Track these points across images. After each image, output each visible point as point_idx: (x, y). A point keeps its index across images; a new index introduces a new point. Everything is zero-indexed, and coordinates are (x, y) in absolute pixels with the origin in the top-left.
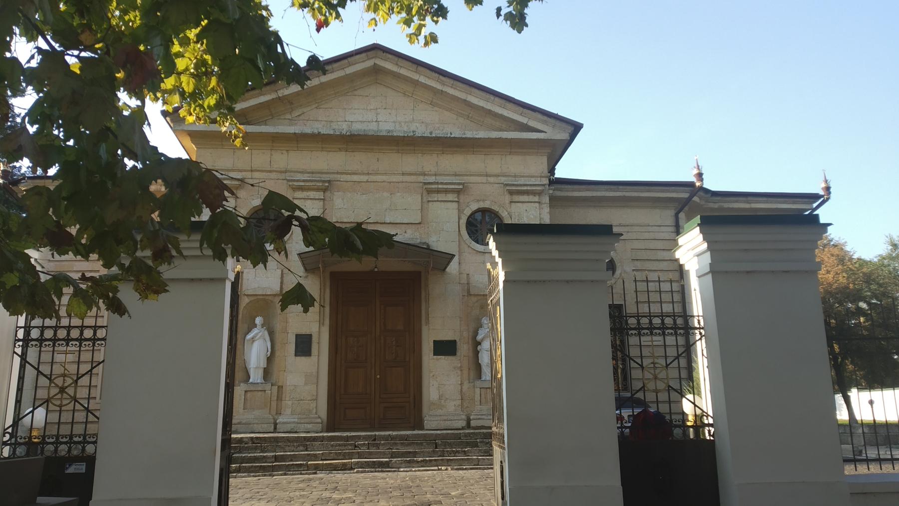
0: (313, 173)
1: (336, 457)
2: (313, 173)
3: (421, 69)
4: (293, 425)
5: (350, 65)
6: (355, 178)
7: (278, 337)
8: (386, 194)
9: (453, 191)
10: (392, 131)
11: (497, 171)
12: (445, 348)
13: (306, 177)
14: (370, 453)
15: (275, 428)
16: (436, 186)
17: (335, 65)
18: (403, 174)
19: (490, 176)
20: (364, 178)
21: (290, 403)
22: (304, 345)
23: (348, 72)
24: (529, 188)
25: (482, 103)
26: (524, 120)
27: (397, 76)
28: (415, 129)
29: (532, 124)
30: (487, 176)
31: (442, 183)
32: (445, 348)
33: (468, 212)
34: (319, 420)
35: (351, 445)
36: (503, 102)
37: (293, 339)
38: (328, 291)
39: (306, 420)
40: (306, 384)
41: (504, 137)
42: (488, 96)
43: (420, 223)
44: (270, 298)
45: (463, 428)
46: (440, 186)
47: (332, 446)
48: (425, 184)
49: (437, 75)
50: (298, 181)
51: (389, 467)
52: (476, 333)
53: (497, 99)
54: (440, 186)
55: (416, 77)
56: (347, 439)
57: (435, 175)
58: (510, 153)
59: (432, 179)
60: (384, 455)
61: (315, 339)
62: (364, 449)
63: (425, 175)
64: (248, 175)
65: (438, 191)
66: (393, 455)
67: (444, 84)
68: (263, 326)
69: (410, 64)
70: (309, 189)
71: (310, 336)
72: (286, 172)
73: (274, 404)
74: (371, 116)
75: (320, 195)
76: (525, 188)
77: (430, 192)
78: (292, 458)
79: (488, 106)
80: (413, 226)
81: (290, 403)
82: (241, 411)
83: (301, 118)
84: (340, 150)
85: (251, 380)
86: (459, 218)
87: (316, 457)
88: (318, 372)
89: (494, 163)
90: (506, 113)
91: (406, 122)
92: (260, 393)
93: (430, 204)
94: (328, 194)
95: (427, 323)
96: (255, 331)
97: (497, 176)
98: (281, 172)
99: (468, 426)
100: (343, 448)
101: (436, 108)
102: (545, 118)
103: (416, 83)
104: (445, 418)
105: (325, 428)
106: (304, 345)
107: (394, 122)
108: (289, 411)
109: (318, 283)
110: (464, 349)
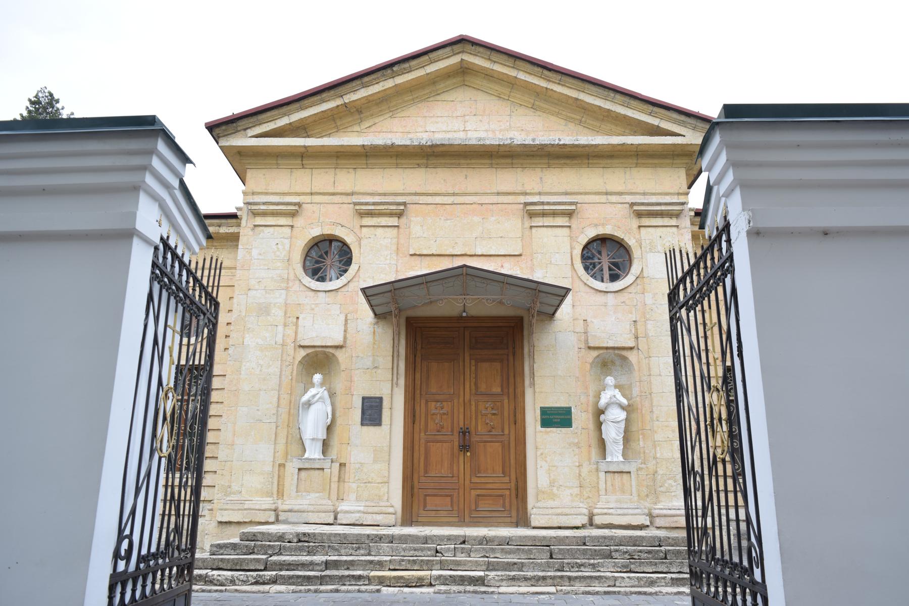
0: (385, 194)
1: (409, 567)
2: (385, 194)
3: (520, 63)
4: (358, 515)
5: (432, 62)
6: (438, 200)
7: (340, 400)
8: (476, 219)
9: (563, 214)
10: (484, 139)
11: (620, 188)
12: (556, 418)
13: (377, 199)
14: (458, 563)
15: (336, 518)
16: (540, 207)
17: (413, 63)
18: (498, 194)
19: (611, 194)
20: (449, 200)
21: (354, 486)
22: (372, 411)
23: (428, 71)
24: (663, 208)
25: (598, 102)
26: (655, 121)
27: (489, 75)
28: (512, 136)
29: (665, 125)
30: (607, 194)
31: (548, 203)
32: (556, 418)
33: (584, 240)
34: (391, 510)
35: (429, 549)
36: (627, 99)
37: (358, 404)
38: (403, 342)
39: (376, 509)
40: (375, 461)
41: (629, 142)
42: (606, 93)
43: (520, 255)
44: (331, 350)
45: (583, 526)
46: (546, 207)
47: (404, 550)
48: (526, 204)
49: (540, 69)
50: (367, 204)
51: (484, 585)
52: (598, 397)
53: (618, 96)
54: (546, 207)
55: (513, 73)
56: (426, 540)
57: (540, 194)
58: (637, 165)
59: (536, 199)
60: (476, 566)
61: (386, 404)
62: (448, 557)
63: (526, 194)
64: (307, 199)
65: (544, 214)
66: (490, 567)
67: (549, 81)
68: (322, 384)
69: (506, 57)
70: (380, 214)
71: (381, 399)
72: (352, 194)
73: (334, 486)
74: (457, 125)
75: (393, 221)
76: (658, 208)
77: (532, 215)
78: (350, 565)
79: (607, 105)
80: (512, 259)
81: (354, 486)
82: (294, 494)
83: (372, 129)
84: (419, 166)
85: (306, 455)
86: (572, 248)
87: (380, 565)
88: (390, 446)
89: (616, 179)
90: (630, 113)
91: (501, 131)
92: (317, 472)
93: (534, 230)
94: (403, 220)
95: (533, 384)
96: (312, 391)
97: (620, 194)
98: (347, 194)
99: (591, 524)
100: (420, 553)
101: (539, 113)
102: (683, 118)
103: (513, 84)
104: (559, 511)
105: (399, 521)
106: (372, 411)
107: (486, 131)
108: (353, 496)
109: (390, 332)
110: (581, 419)
